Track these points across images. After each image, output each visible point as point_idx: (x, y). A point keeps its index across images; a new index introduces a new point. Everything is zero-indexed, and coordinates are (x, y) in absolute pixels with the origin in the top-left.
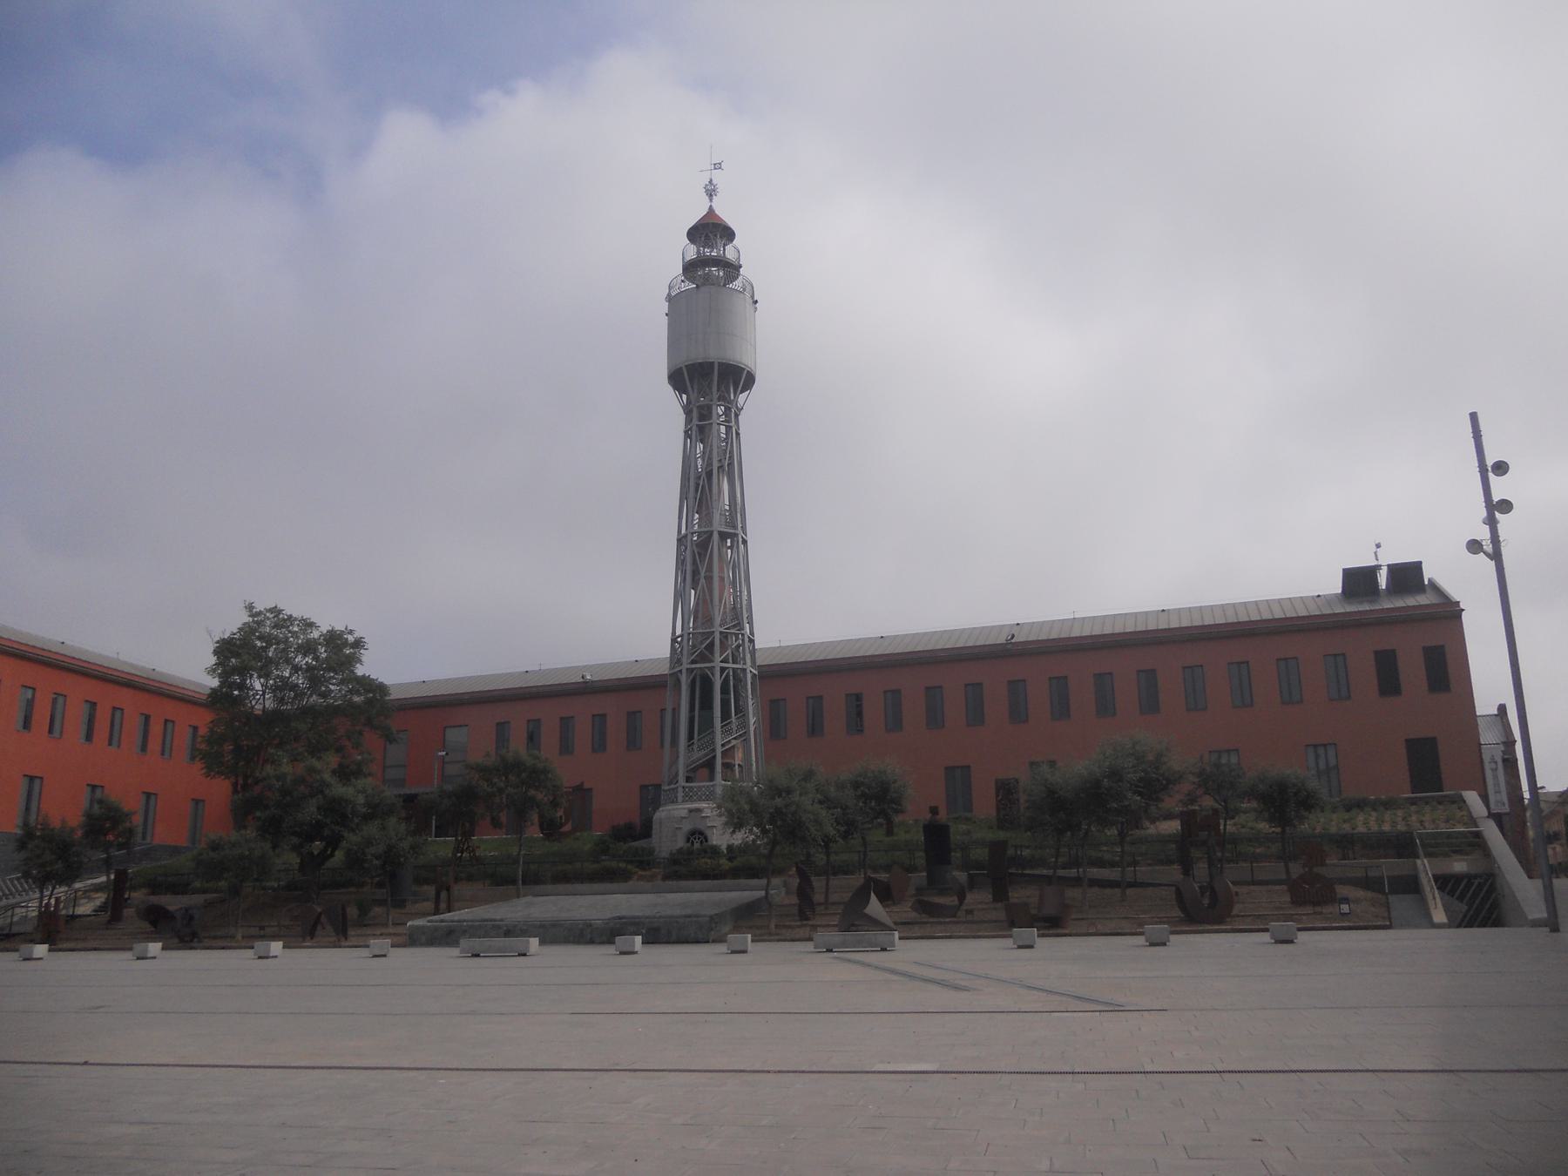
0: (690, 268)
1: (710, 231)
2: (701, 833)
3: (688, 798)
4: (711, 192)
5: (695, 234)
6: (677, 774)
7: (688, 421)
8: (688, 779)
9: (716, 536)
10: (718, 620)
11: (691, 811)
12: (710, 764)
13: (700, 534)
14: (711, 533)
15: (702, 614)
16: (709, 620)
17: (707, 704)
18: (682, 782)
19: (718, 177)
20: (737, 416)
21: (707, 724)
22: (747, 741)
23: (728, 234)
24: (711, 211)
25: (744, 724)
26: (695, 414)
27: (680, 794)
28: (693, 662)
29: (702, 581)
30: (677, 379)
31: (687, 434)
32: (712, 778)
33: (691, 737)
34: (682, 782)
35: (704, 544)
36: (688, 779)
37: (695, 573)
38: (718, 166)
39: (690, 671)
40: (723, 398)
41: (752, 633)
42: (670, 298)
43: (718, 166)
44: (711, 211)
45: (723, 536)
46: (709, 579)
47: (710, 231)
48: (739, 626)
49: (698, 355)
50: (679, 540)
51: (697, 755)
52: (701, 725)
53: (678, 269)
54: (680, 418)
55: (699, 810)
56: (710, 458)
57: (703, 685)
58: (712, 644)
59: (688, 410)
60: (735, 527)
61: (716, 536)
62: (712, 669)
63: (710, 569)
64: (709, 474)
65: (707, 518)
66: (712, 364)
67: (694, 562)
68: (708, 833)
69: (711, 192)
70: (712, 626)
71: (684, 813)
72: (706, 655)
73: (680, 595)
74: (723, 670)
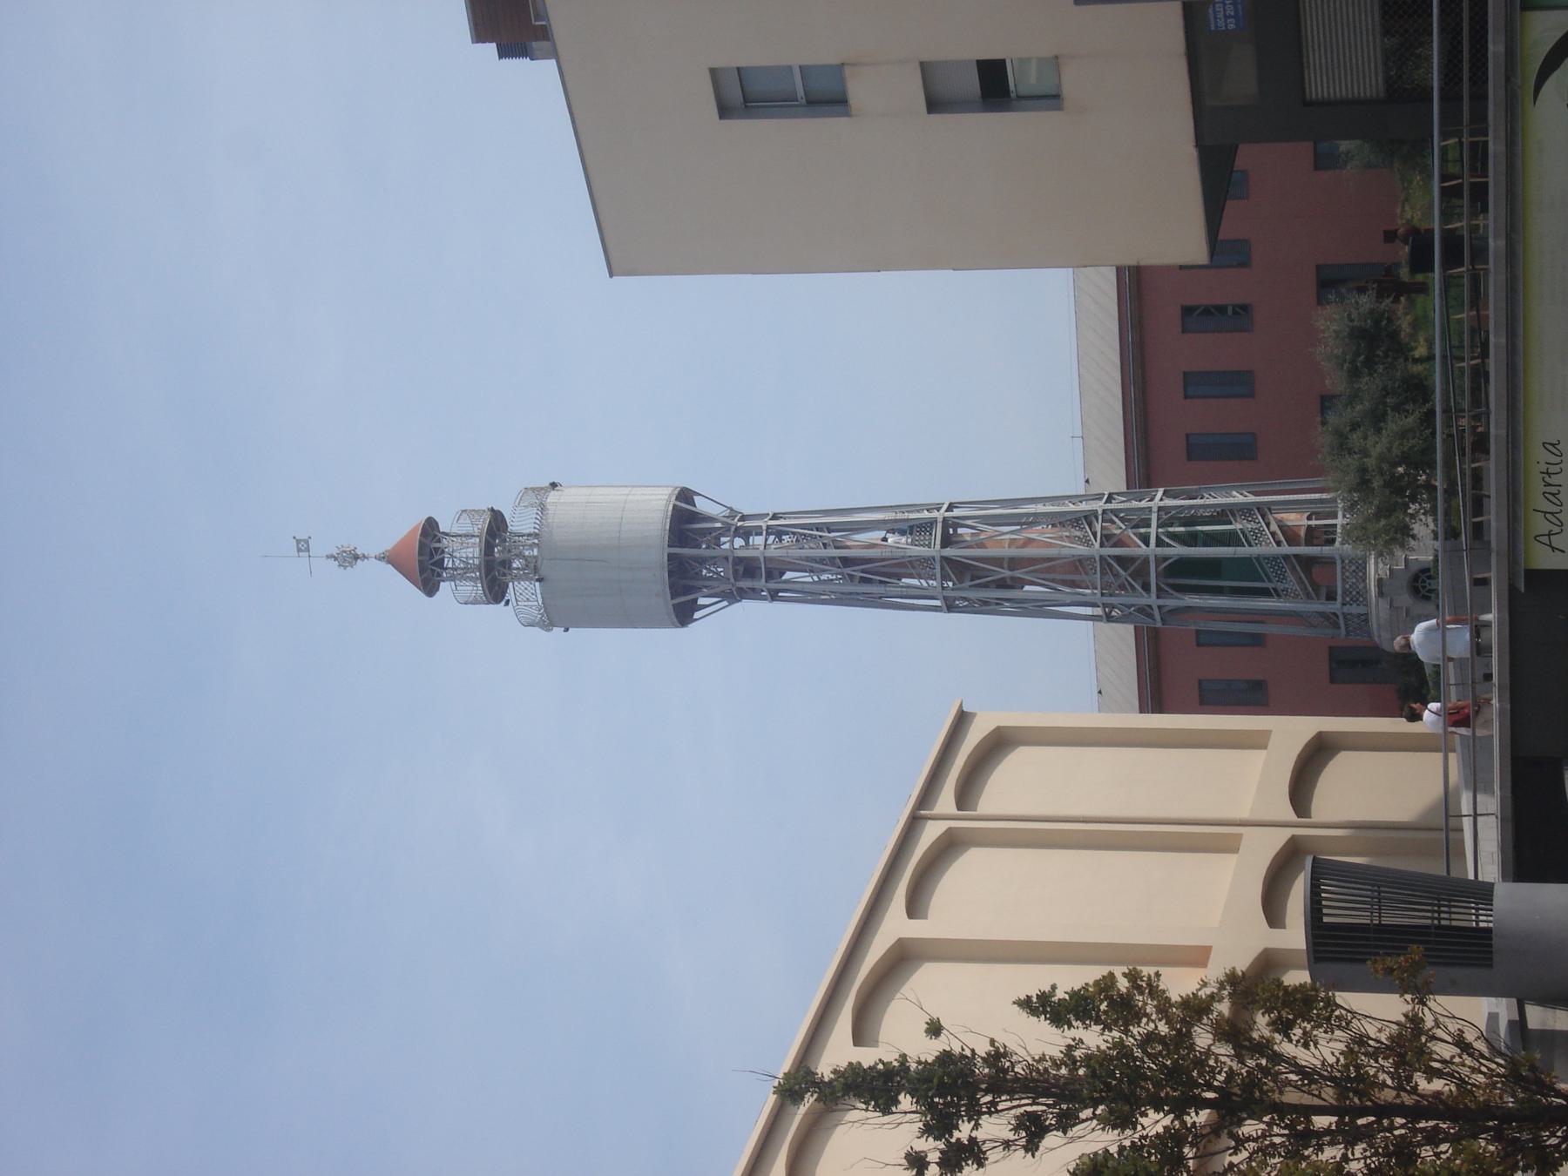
1: (425, 561)
2: (1416, 578)
3: (1358, 596)
4: (350, 558)
6: (1322, 614)
7: (753, 594)
8: (1331, 597)
9: (949, 552)
10: (1081, 550)
11: (1381, 594)
12: (1307, 563)
13: (945, 577)
14: (945, 559)
15: (1068, 574)
16: (1079, 564)
17: (1212, 567)
18: (1335, 607)
20: (743, 518)
21: (1246, 567)
22: (1269, 505)
23: (430, 528)
25: (1245, 511)
26: (746, 584)
27: (1354, 609)
28: (1146, 587)
29: (1017, 574)
30: (684, 615)
31: (774, 596)
32: (1329, 562)
33: (1265, 593)
34: (1335, 607)
35: (957, 569)
36: (1331, 597)
37: (1002, 584)
38: (303, 546)
39: (1161, 593)
40: (714, 537)
41: (1099, 497)
42: (548, 623)
43: (303, 546)
45: (947, 541)
46: (1014, 563)
47: (425, 561)
48: (1089, 517)
49: (658, 578)
50: (950, 607)
51: (1291, 583)
52: (1246, 576)
54: (750, 611)
55: (1380, 582)
56: (822, 561)
57: (1181, 574)
58: (1118, 559)
60: (933, 522)
61: (949, 552)
62: (1160, 560)
63: (998, 561)
64: (846, 562)
65: (918, 566)
66: (670, 555)
67: (985, 586)
68: (1414, 568)
69: (350, 558)
70: (1091, 558)
71: (1384, 605)
72: (1136, 569)
73: (1037, 609)
74: (1160, 543)
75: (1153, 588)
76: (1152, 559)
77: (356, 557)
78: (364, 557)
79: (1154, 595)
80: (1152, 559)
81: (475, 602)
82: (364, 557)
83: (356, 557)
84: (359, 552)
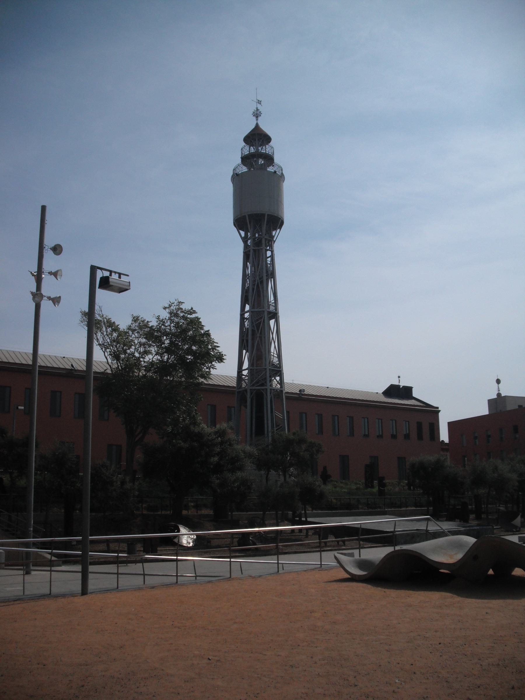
0: (245, 159)
1: (257, 138)
4: (257, 114)
5: (250, 139)
9: (266, 313)
19: (259, 107)
24: (257, 126)
28: (253, 385)
30: (240, 223)
44: (257, 126)
47: (257, 138)
53: (239, 161)
57: (259, 398)
59: (245, 240)
66: (263, 215)
69: (257, 114)
75: (254, 388)
76: (266, 387)
77: (257, 117)
78: (257, 120)
79: (251, 388)
80: (266, 387)
81: (242, 154)
82: (257, 120)
83: (257, 117)
84: (259, 118)
